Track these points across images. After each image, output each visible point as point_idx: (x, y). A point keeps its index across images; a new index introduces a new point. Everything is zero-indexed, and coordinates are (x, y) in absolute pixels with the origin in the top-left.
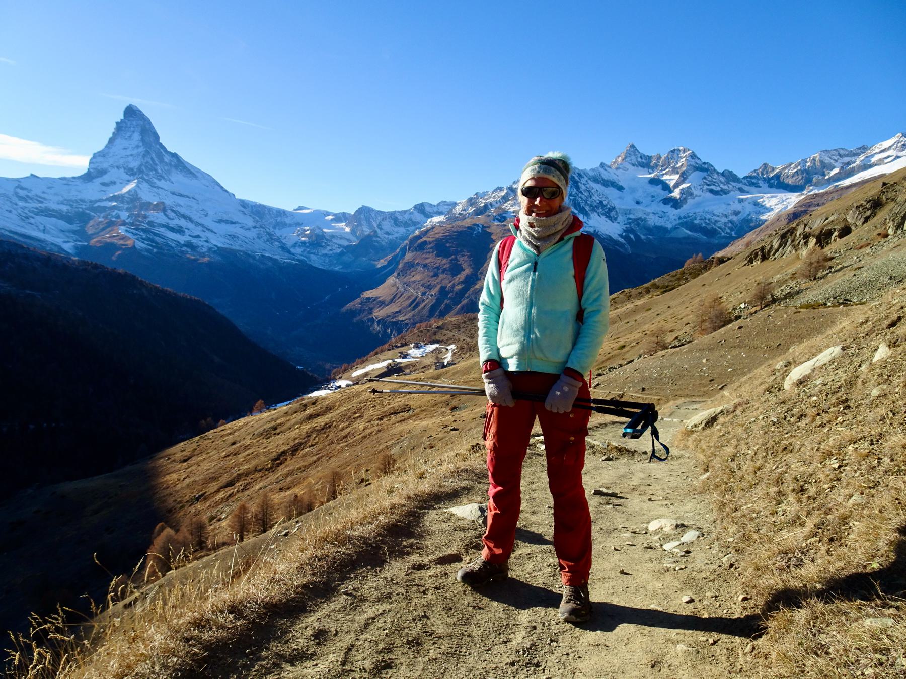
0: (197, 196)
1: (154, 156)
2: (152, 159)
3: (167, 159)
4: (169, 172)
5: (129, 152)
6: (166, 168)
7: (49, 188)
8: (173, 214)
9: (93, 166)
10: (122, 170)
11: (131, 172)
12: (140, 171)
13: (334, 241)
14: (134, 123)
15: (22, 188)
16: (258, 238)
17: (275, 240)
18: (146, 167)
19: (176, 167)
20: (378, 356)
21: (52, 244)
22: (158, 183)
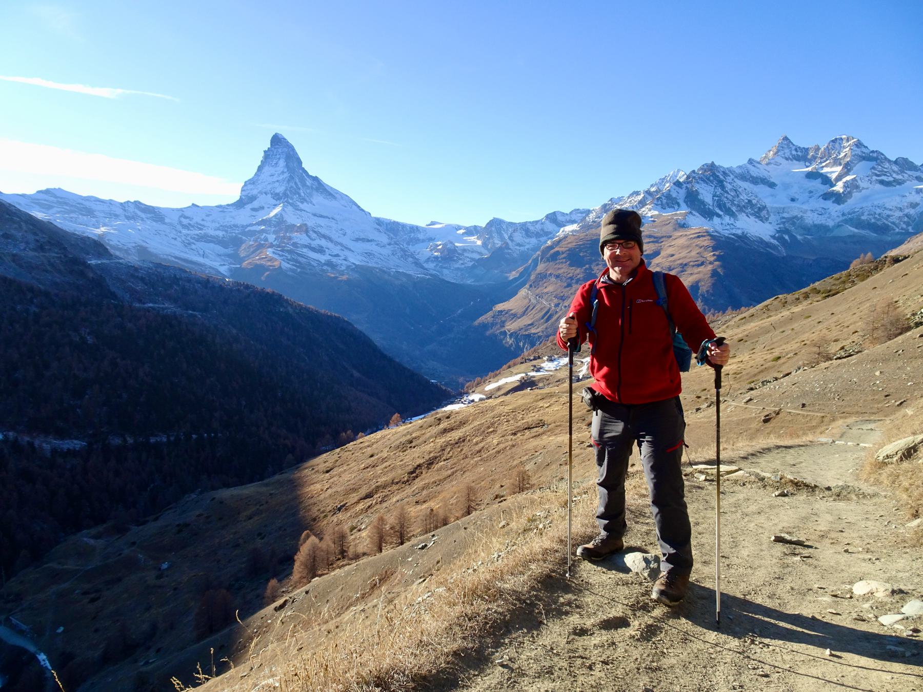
0: (336, 217)
2: (296, 183)
3: (309, 182)
4: (311, 195)
5: (275, 179)
7: (208, 216)
9: (244, 193)
10: (269, 196)
11: (277, 197)
12: (285, 195)
13: (466, 254)
14: (280, 150)
15: (186, 217)
18: (291, 191)
19: (317, 190)
20: (511, 369)
21: (210, 267)
22: (302, 206)
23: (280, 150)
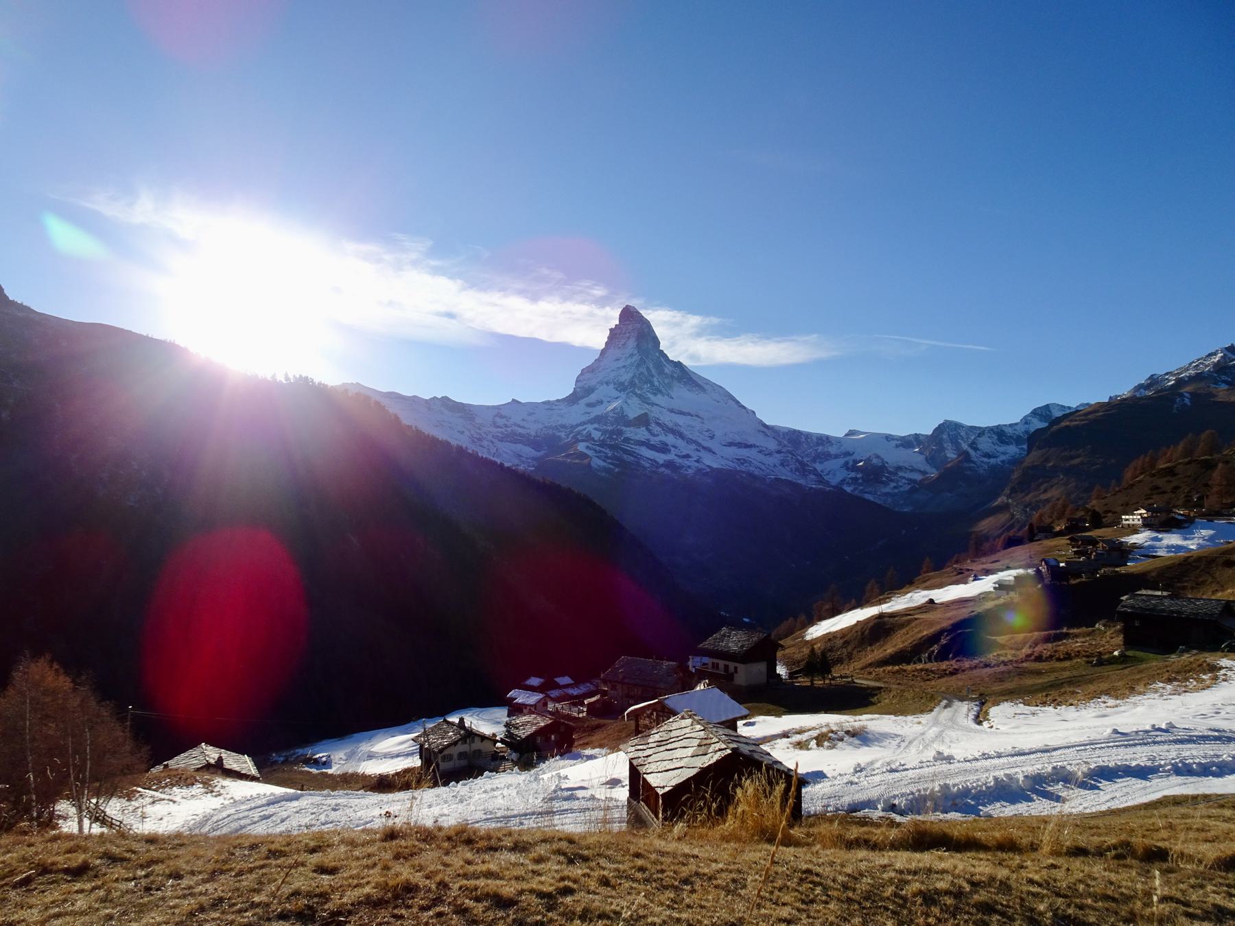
1: (651, 366)
2: (648, 368)
3: (668, 369)
4: (670, 386)
6: (666, 381)
7: (530, 414)
8: (659, 429)
9: (580, 384)
10: (612, 386)
11: (621, 387)
12: (632, 384)
13: (901, 474)
14: (630, 327)
15: (502, 417)
16: (782, 464)
17: (810, 472)
19: (679, 379)
23: (630, 327)
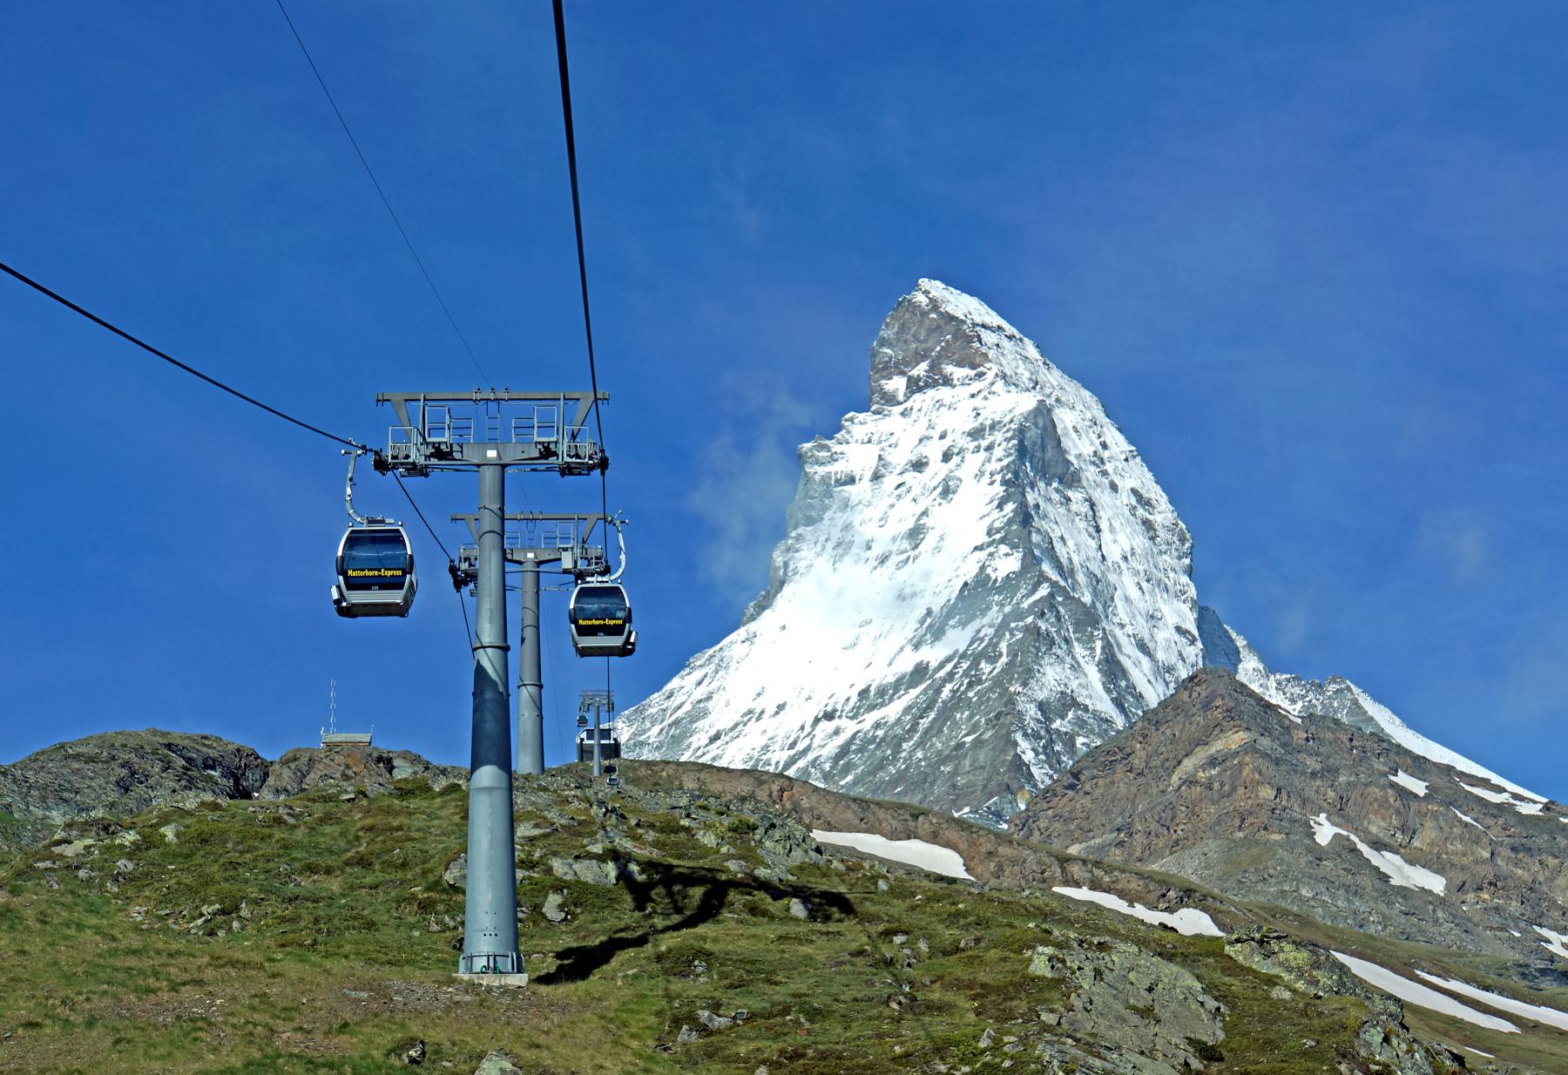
23: (958, 421)
